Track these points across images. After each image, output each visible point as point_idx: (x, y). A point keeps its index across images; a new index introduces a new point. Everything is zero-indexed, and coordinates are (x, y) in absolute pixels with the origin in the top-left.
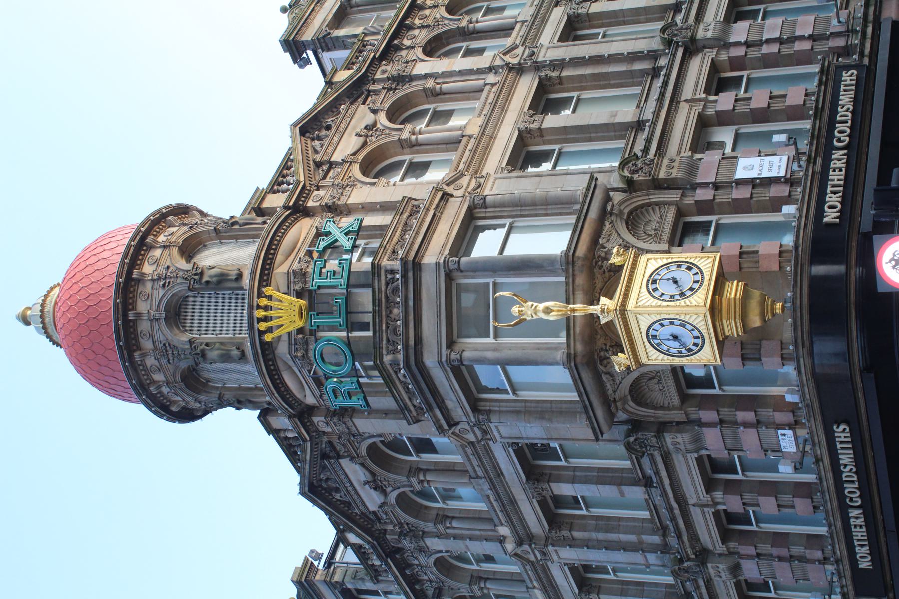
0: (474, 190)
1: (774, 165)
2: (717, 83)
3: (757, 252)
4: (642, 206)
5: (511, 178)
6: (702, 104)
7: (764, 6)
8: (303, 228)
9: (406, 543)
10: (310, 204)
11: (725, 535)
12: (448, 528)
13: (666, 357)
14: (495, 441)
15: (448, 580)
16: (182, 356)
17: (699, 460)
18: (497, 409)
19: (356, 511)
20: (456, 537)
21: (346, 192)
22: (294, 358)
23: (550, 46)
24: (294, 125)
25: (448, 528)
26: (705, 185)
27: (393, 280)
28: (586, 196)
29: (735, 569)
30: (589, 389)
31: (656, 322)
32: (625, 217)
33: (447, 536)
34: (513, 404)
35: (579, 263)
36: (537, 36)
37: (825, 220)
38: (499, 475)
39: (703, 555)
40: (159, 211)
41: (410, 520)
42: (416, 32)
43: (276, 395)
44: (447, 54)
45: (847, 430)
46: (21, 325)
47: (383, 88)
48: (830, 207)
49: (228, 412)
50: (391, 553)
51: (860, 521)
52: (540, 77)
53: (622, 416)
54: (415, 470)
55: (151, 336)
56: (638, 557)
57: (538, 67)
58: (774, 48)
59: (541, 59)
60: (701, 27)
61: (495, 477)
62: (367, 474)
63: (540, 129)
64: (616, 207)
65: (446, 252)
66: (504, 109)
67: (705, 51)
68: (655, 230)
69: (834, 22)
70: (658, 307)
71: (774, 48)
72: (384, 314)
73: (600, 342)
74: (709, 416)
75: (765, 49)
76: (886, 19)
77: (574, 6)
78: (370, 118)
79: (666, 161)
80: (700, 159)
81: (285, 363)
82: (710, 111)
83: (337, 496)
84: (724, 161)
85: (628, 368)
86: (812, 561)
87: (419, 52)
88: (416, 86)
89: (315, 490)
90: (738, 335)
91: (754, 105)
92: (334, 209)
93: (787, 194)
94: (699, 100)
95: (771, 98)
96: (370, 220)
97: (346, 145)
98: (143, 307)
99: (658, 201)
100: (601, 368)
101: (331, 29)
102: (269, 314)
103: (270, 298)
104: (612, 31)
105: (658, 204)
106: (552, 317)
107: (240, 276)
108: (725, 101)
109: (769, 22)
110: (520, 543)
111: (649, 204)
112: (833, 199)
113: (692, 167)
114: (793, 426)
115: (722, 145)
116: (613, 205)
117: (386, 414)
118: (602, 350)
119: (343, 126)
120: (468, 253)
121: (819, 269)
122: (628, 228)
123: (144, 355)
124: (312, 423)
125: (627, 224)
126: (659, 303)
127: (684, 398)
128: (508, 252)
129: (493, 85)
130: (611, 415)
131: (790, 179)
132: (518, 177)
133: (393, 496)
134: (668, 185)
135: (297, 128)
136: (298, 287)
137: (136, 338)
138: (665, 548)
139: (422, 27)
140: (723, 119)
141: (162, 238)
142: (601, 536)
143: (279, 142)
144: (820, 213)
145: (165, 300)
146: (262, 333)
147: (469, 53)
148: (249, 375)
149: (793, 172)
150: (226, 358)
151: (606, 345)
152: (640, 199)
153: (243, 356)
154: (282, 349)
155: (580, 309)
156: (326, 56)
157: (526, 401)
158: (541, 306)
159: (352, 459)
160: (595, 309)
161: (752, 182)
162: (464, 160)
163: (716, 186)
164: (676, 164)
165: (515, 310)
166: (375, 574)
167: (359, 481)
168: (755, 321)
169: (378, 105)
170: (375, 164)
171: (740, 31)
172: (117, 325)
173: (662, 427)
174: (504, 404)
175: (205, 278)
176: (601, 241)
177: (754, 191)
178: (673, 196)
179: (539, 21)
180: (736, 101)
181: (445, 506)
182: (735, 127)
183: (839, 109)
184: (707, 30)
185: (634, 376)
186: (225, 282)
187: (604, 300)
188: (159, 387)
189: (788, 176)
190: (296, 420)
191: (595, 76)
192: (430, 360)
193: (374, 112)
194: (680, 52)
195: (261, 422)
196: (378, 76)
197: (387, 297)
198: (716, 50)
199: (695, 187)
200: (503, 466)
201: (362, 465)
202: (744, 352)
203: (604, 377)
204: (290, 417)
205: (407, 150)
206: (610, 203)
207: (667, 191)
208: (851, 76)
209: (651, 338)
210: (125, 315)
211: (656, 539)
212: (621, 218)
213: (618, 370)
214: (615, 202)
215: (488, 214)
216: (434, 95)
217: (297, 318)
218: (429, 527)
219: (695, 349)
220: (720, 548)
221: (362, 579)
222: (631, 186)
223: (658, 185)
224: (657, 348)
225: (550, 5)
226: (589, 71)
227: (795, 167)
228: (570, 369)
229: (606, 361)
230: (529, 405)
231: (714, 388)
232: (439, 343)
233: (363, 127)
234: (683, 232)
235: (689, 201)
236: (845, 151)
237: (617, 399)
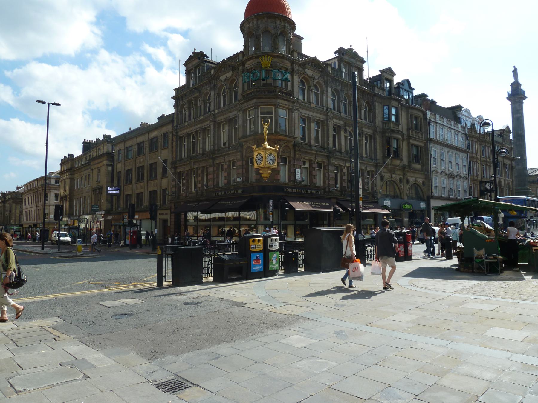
1: (298, 177)
8: (288, 64)
20: (214, 99)
29: (210, 166)
33: (214, 96)
36: (336, 118)
39: (213, 159)
56: (212, 143)
57: (327, 120)
58: (327, 175)
66: (316, 113)
74: (244, 163)
78: (317, 77)
96: (289, 84)
99: (292, 151)
110: (214, 115)
112: (290, 190)
134: (295, 154)
138: (214, 150)
141: (286, 24)
142: (216, 135)
144: (287, 187)
155: (266, 138)
156: (336, 60)
163: (294, 165)
165: (266, 124)
178: (292, 155)
179: (340, 119)
184: (333, 161)
186: (275, 47)
199: (294, 160)
209: (259, 154)
211: (216, 148)
218: (216, 92)
224: (257, 155)
226: (325, 133)
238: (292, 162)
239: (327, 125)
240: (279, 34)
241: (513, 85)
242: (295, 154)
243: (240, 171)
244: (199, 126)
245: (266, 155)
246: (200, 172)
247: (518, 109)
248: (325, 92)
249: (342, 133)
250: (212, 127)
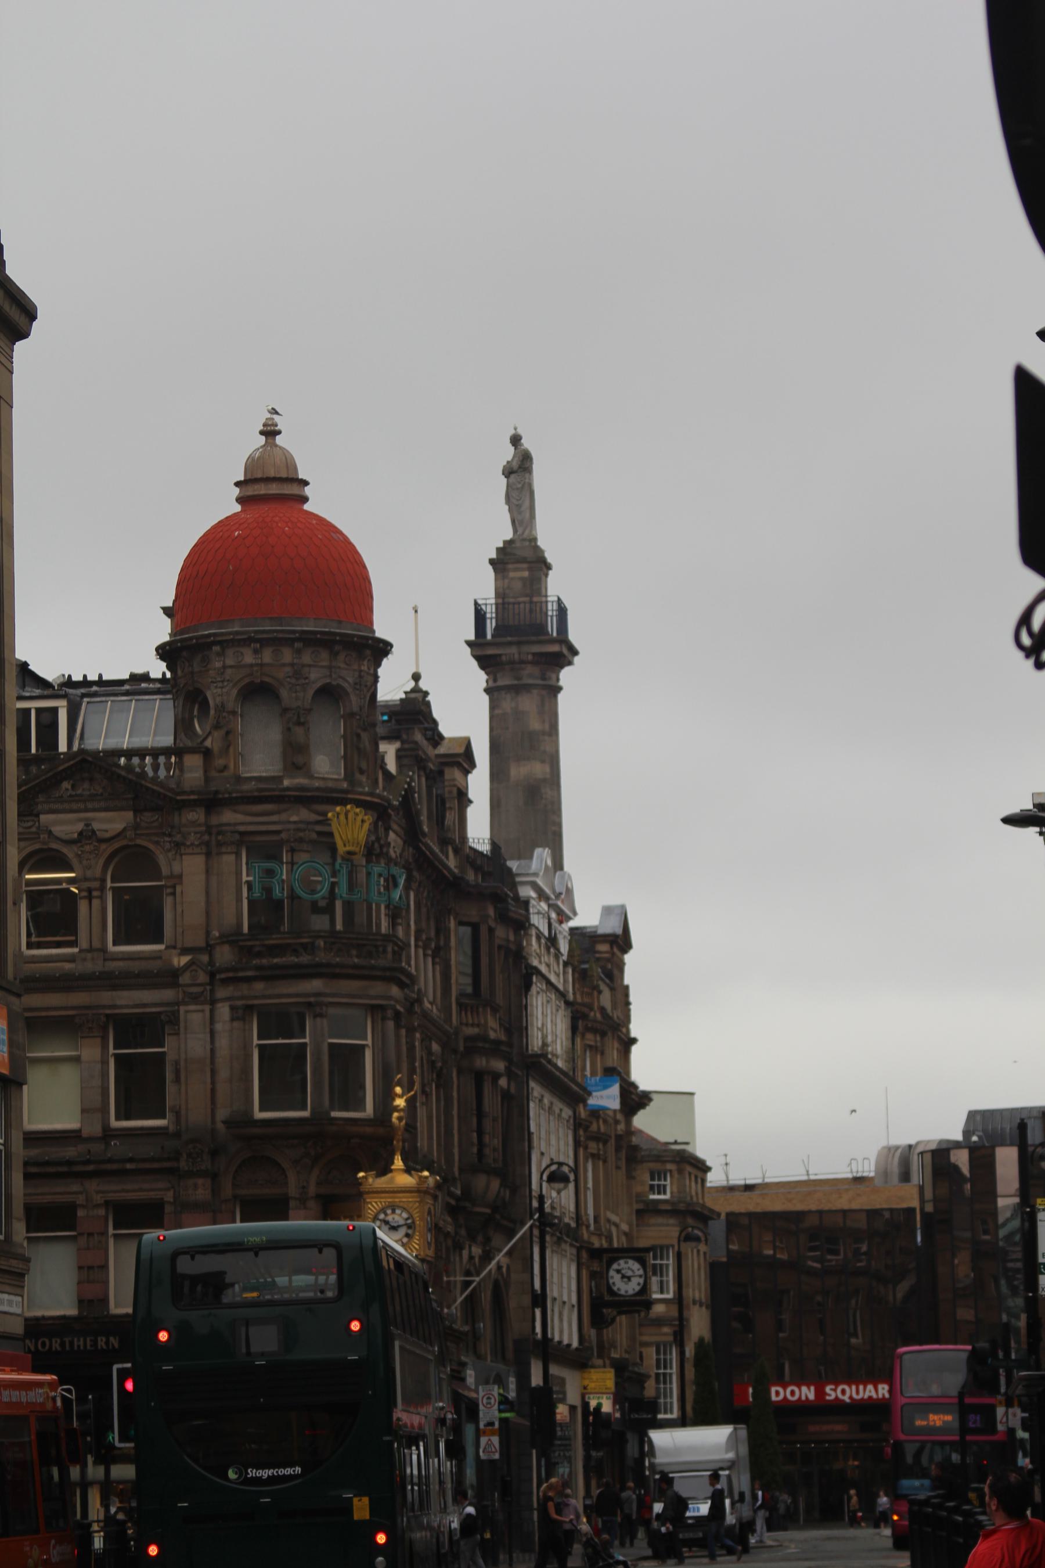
43: (256, 794)
83: (66, 785)
145: (345, 685)
167: (93, 819)
173: (214, 1176)
200: (125, 994)
217: (348, 848)
241: (503, 561)
247: (535, 725)
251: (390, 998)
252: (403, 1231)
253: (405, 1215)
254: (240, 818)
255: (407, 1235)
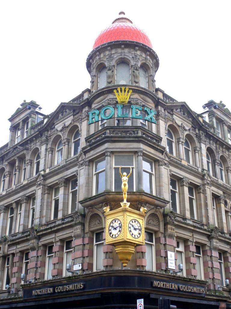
0: (164, 162)
1: (172, 265)
2: (199, 247)
3: (143, 258)
4: (158, 219)
5: (168, 174)
6: (192, 240)
7: (223, 262)
9: (44, 138)
10: (159, 107)
11: (45, 246)
12: (49, 152)
13: (109, 225)
14: (79, 168)
15: (31, 152)
16: (109, 63)
17: (71, 237)
18: (90, 168)
19: (55, 122)
20: (46, 155)
21: (163, 119)
22: (108, 100)
23: (210, 190)
24: (185, 103)
25: (49, 152)
26: (166, 241)
27: (134, 133)
28: (162, 199)
29: (33, 249)
30: (97, 199)
31: (121, 222)
32: (155, 213)
34: (91, 173)
35: (140, 197)
37: (155, 281)
38: (67, 169)
40: (157, 57)
41: (52, 140)
42: (215, 145)
44: (207, 155)
45: (81, 288)
46: (120, 12)
47: (197, 133)
48: (159, 283)
49: (90, 79)
50: (40, 133)
51: (49, 292)
52: (201, 186)
53: (87, 211)
54: (68, 141)
55: (116, 53)
57: (204, 185)
59: (206, 186)
60: (217, 241)
61: (65, 168)
62: (67, 125)
63: (184, 185)
64: (158, 210)
65: (144, 152)
66: (190, 173)
67: (209, 242)
68: (151, 223)
69: (219, 286)
70: (127, 223)
71: (210, 265)
72: (123, 130)
73: (113, 203)
74: (86, 241)
75: (210, 263)
76: (220, 304)
77: (223, 198)
79: (173, 227)
80: (174, 239)
81: (106, 97)
82: (189, 243)
83: (60, 115)
84: (173, 247)
85: (104, 212)
86: (35, 275)
87: (208, 146)
88: (197, 144)
89: (63, 108)
90: (116, 251)
91: (192, 258)
92: (158, 115)
93: (162, 269)
94: (193, 240)
95: (194, 264)
97: (178, 121)
98: (126, 50)
100: (104, 204)
101: (216, 117)
102: (123, 91)
103: (128, 92)
104: (215, 211)
105: (159, 224)
106: (123, 186)
107: (136, 83)
108: (193, 248)
109: (218, 264)
110: (43, 176)
111: (159, 221)
112: (161, 285)
113: (171, 236)
114: (83, 270)
115: (178, 246)
116: (159, 209)
117: (88, 131)
118: (110, 204)
119: (185, 119)
120: (144, 160)
121: (136, 278)
122: (151, 214)
123: (109, 50)
124: (85, 106)
125: (153, 214)
126: (128, 223)
127: (92, 232)
128: (144, 173)
129: (198, 170)
130: (87, 207)
131: (167, 270)
132: (168, 177)
133: (60, 134)
134: (165, 229)
135: (184, 104)
136: (132, 102)
137: (115, 48)
139: (216, 147)
140: (187, 247)
141: (148, 57)
142: (45, 204)
143: (179, 98)
144: (157, 280)
146: (116, 89)
147: (208, 162)
148: (103, 84)
149: (170, 271)
150: (109, 77)
151: (112, 205)
152: (161, 218)
153: (110, 83)
154: (111, 96)
155: (125, 196)
157: (92, 178)
158: (126, 183)
159: (73, 120)
160: (125, 201)
161: (166, 257)
162: (174, 159)
164: (173, 231)
165: (125, 174)
166: (32, 128)
167: (65, 122)
168: (120, 256)
169: (191, 131)
170: (172, 130)
171: (215, 254)
172: (120, 41)
173: (83, 225)
174: (92, 171)
175: (135, 71)
176: (147, 204)
177: (163, 258)
178: (162, 230)
179: (218, 186)
180: (193, 252)
181: (56, 151)
182: (184, 252)
183: (192, 287)
185: (101, 215)
187: (129, 204)
188: (99, 56)
189: (168, 269)
190: (87, 101)
191: (201, 205)
192: (106, 145)
193: (189, 130)
194: (209, 234)
195: (86, 89)
196: (201, 132)
197: (129, 131)
198: (209, 245)
199: (165, 237)
201: (71, 123)
202: (109, 253)
203: (101, 204)
204: (88, 99)
205: (177, 141)
206: (160, 208)
207: (163, 227)
208: (203, 291)
210: (123, 44)
212: (155, 212)
213: (104, 208)
214: (160, 210)
215: (156, 166)
216: (195, 150)
218: (49, 146)
219: (111, 235)
220: (40, 244)
221: (32, 124)
222: (165, 215)
223: (166, 224)
225: (223, 190)
226: (203, 203)
227: (171, 272)
228: (104, 193)
229: (106, 205)
230: (91, 179)
231: (96, 242)
232: (113, 148)
233: (184, 126)
234: (150, 234)
235: (160, 235)
236: (177, 289)
237: (93, 209)
238: (162, 241)
239: (204, 192)
240: (139, 66)
242: (165, 229)
243: (79, 254)
244: (21, 194)
245: (126, 226)
246: (16, 259)
248: (198, 149)
249: (223, 206)
250: (39, 193)
251: (140, 148)
252: (118, 229)
253: (119, 222)
254: (96, 105)
255: (120, 231)
